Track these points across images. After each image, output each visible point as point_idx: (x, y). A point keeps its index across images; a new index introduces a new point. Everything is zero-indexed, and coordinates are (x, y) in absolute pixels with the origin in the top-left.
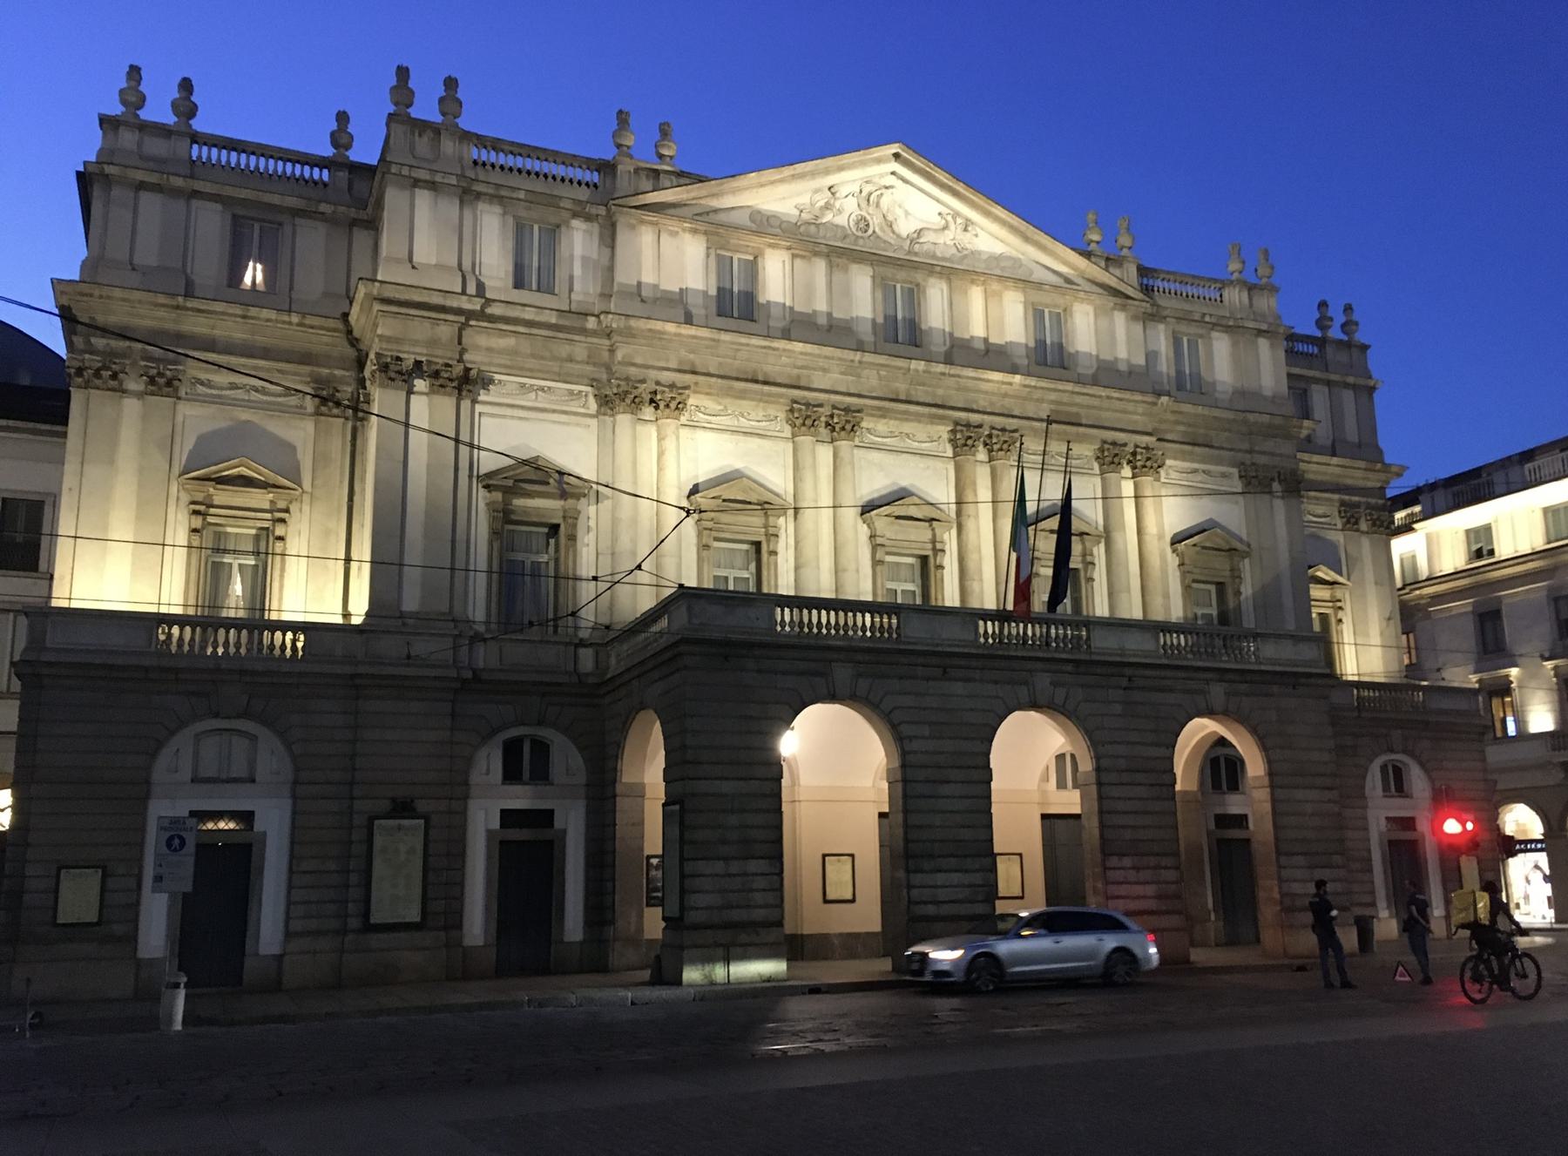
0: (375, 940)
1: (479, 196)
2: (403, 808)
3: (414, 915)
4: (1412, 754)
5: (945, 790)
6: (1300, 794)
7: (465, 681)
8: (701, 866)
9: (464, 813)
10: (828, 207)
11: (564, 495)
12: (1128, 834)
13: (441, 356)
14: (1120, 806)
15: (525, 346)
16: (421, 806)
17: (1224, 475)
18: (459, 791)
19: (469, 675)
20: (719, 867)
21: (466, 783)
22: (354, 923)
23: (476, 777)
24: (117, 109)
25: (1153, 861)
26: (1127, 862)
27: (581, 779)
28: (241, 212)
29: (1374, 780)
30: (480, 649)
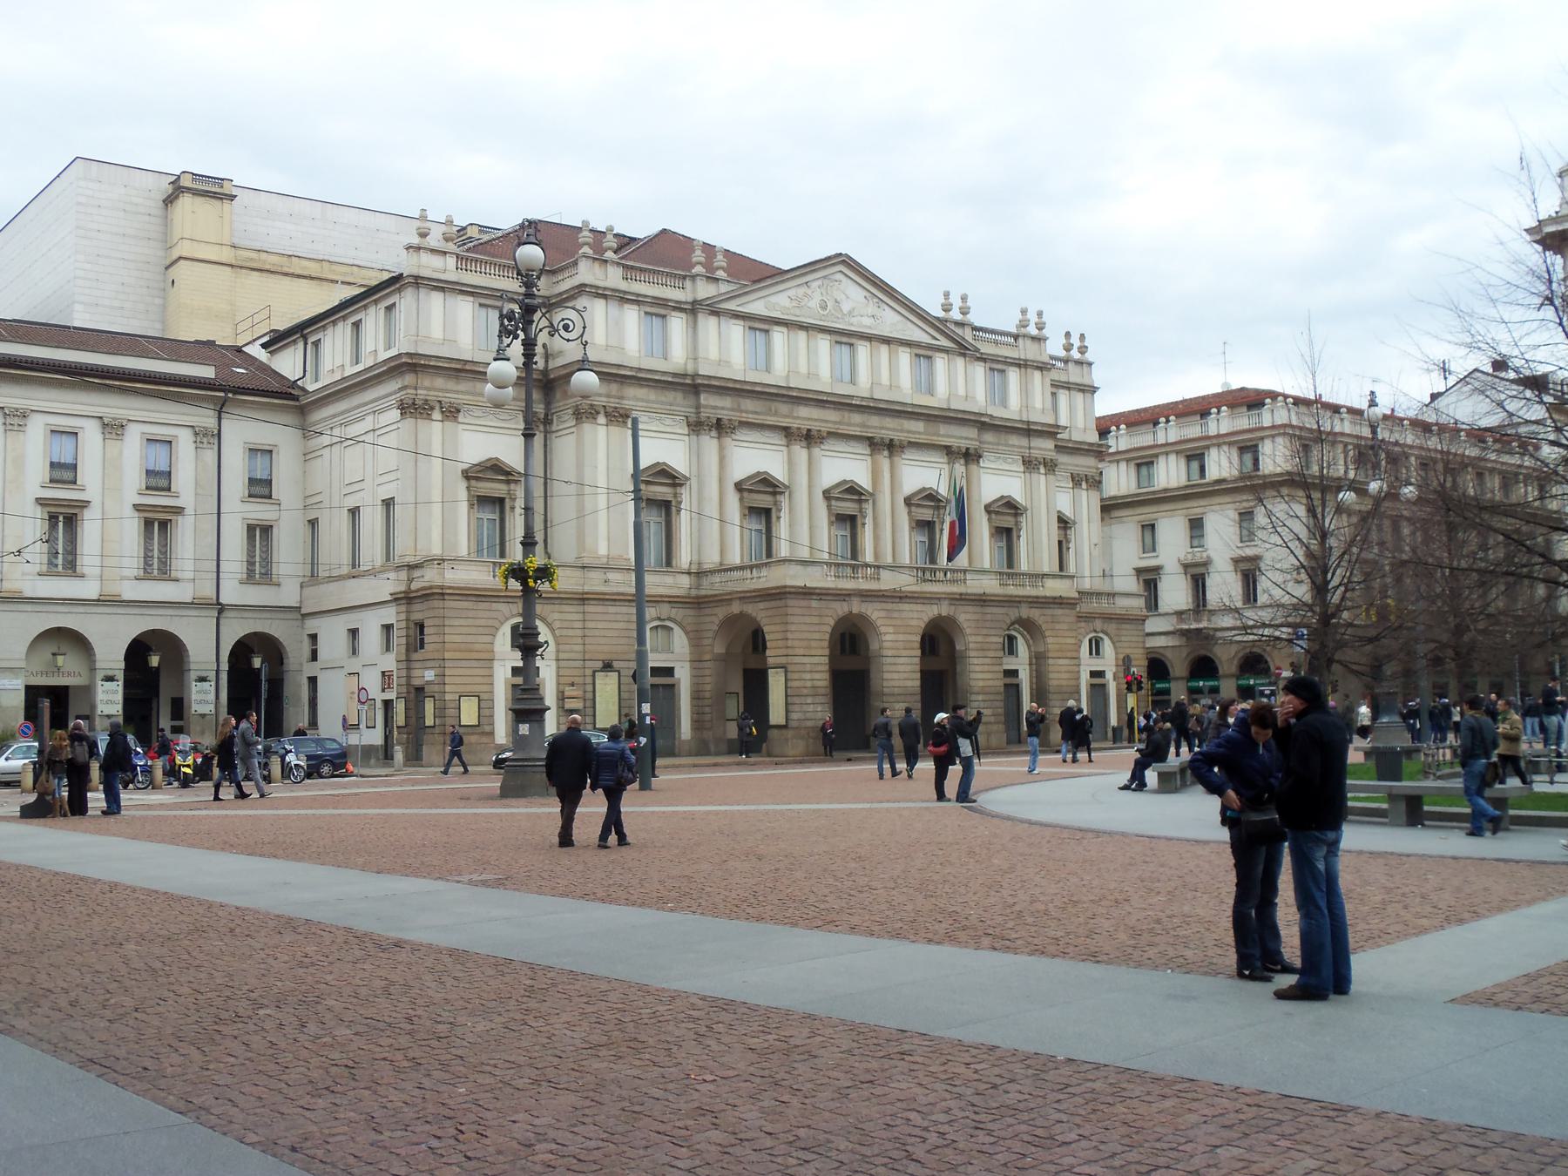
2: (608, 667)
4: (1106, 634)
5: (902, 660)
6: (1061, 662)
8: (796, 700)
10: (806, 295)
11: (674, 485)
12: (981, 684)
13: (613, 402)
14: (978, 668)
16: (616, 664)
20: (803, 700)
24: (416, 240)
26: (980, 698)
27: (687, 650)
28: (483, 301)
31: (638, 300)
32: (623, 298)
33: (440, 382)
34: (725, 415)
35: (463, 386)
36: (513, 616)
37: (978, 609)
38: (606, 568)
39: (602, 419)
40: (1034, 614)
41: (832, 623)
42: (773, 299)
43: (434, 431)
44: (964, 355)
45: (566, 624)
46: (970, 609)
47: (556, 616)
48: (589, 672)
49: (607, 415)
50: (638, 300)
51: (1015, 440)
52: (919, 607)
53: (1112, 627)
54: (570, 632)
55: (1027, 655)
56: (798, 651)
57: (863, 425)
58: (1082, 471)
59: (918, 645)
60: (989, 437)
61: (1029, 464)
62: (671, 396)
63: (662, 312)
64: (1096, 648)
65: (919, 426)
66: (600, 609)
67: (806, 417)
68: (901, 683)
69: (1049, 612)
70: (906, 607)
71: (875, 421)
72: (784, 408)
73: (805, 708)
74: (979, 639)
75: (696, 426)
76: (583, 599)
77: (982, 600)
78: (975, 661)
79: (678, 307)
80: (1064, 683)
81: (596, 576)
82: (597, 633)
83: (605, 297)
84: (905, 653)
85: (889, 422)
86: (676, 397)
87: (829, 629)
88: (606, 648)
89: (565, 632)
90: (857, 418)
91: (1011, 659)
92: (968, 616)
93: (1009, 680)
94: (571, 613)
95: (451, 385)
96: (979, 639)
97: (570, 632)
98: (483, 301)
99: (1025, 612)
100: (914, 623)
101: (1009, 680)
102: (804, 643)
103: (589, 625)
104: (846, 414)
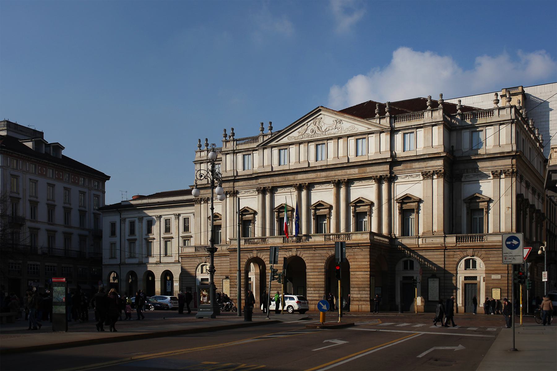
2: (227, 278)
6: (358, 273)
14: (311, 277)
17: (417, 176)
25: (318, 289)
26: (312, 289)
37: (313, 252)
46: (308, 252)
51: (416, 165)
53: (483, 252)
61: (427, 175)
66: (224, 259)
74: (312, 264)
78: (310, 274)
82: (224, 267)
92: (307, 255)
96: (312, 264)
103: (222, 264)
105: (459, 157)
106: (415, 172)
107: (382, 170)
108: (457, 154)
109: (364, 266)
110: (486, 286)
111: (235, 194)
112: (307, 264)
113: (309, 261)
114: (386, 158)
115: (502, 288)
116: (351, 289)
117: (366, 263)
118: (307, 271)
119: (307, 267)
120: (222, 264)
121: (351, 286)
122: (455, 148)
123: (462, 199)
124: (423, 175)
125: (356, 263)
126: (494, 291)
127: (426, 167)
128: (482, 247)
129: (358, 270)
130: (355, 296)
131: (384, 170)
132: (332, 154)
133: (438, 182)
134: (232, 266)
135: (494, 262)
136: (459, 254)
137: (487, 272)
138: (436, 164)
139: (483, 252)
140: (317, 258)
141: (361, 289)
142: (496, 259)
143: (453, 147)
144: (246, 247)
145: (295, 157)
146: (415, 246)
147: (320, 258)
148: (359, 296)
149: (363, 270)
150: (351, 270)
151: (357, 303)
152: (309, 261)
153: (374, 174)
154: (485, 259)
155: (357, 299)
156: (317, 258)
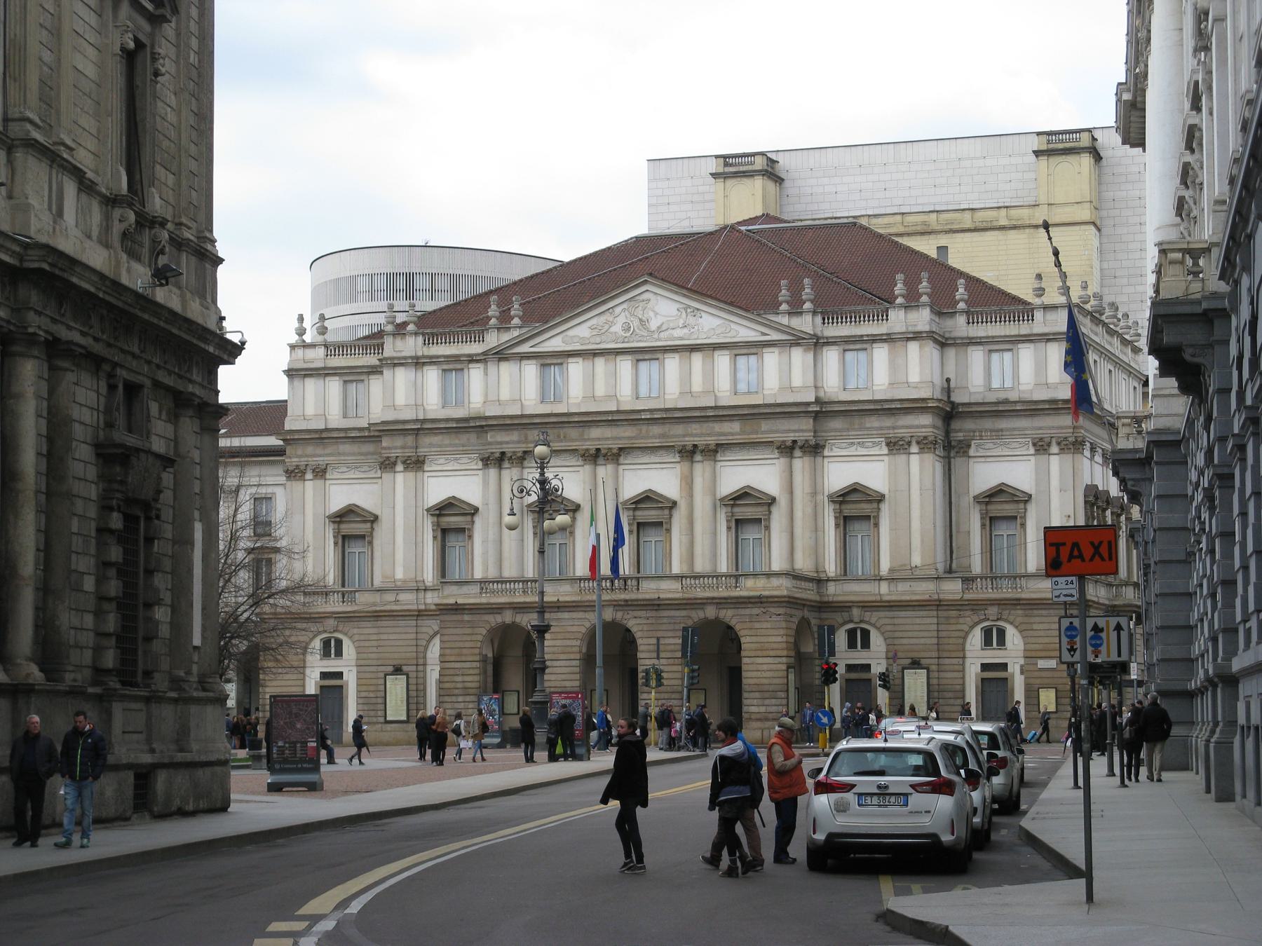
0: (389, 727)
1: (424, 364)
2: (398, 670)
3: (404, 718)
4: (1006, 621)
7: (419, 611)
8: (447, 699)
9: (425, 671)
15: (446, 440)
16: (405, 668)
18: (421, 663)
19: (422, 607)
20: (454, 699)
21: (425, 657)
22: (382, 720)
23: (429, 655)
24: (294, 338)
28: (347, 378)
29: (976, 637)
30: (429, 594)
31: (433, 361)
32: (418, 363)
33: (310, 449)
34: (508, 449)
35: (328, 451)
36: (320, 633)
38: (398, 590)
39: (400, 467)
40: (727, 615)
41: (484, 632)
42: (570, 333)
43: (310, 486)
44: (798, 344)
45: (362, 637)
46: (642, 613)
47: (355, 631)
48: (382, 675)
49: (404, 463)
50: (433, 361)
51: (873, 422)
52: (581, 615)
54: (367, 644)
55: (883, 648)
56: (448, 658)
57: (663, 436)
58: (1045, 433)
59: (577, 649)
60: (836, 424)
61: (896, 446)
62: (464, 438)
63: (459, 366)
64: (994, 637)
65: (735, 426)
67: (599, 436)
68: (557, 684)
69: (747, 611)
70: (566, 615)
71: (679, 429)
72: (573, 433)
73: (457, 706)
75: (486, 461)
76: (377, 616)
77: (656, 605)
79: (472, 359)
80: (766, 681)
81: (390, 597)
83: (402, 364)
84: (563, 656)
85: (695, 428)
86: (473, 437)
87: (480, 638)
88: (396, 656)
89: (362, 644)
90: (656, 430)
91: (864, 653)
92: (638, 621)
93: (853, 676)
94: (368, 629)
95: (319, 451)
97: (367, 644)
98: (347, 378)
99: (710, 612)
100: (575, 629)
101: (853, 676)
102: (456, 651)
104: (644, 428)
105: (964, 404)
106: (869, 436)
107: (795, 427)
108: (958, 398)
109: (775, 646)
110: (1026, 684)
111: (416, 464)
112: (639, 642)
113: (646, 634)
114: (808, 404)
115: (1060, 687)
116: (745, 695)
117: (779, 639)
118: (640, 655)
119: (640, 648)
120: (385, 637)
121: (745, 687)
122: (953, 384)
123: (972, 495)
124: (888, 444)
125: (754, 639)
126: (1043, 693)
127: (894, 428)
128: (1016, 603)
129: (759, 653)
130: (753, 709)
131: (801, 429)
132: (674, 384)
133: (921, 462)
134: (448, 645)
135: (1042, 633)
136: (969, 617)
137: (1029, 654)
138: (916, 422)
139: (1020, 612)
140: (664, 627)
141: (767, 695)
142: (1046, 626)
143: (948, 380)
144: (484, 601)
145: (580, 387)
146: (873, 598)
147: (671, 627)
148: (763, 709)
149: (772, 653)
150: (743, 653)
151: (759, 724)
152: (646, 634)
153: (778, 437)
154: (1024, 627)
155: (758, 716)
156: (664, 627)
